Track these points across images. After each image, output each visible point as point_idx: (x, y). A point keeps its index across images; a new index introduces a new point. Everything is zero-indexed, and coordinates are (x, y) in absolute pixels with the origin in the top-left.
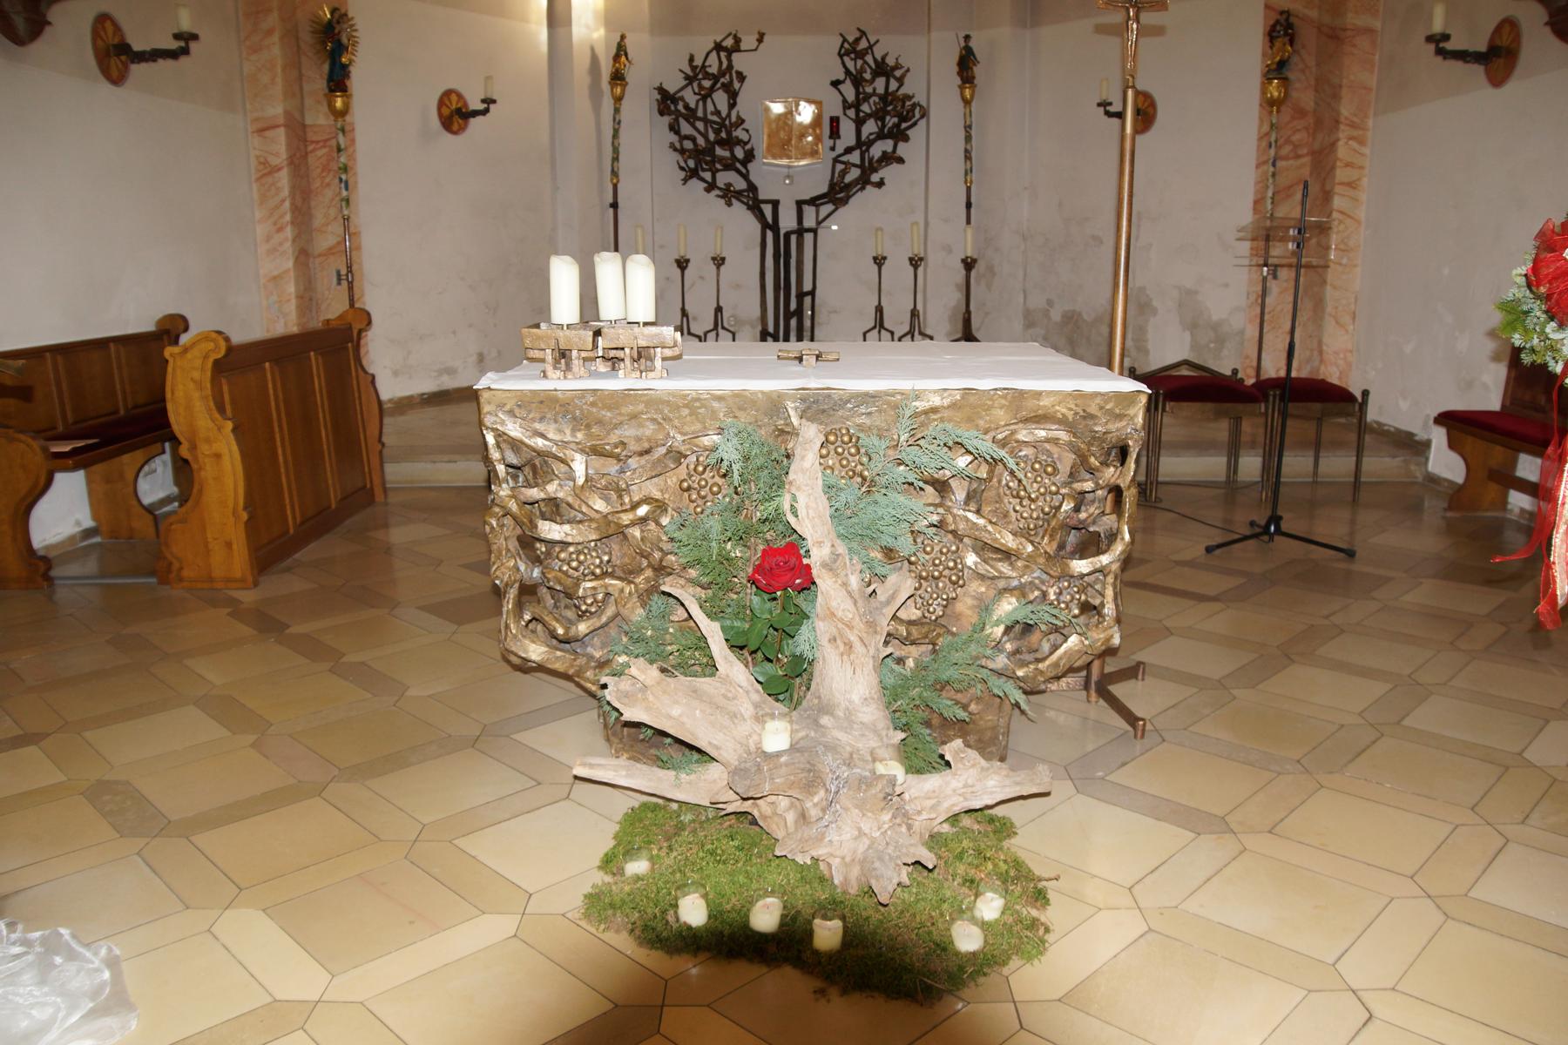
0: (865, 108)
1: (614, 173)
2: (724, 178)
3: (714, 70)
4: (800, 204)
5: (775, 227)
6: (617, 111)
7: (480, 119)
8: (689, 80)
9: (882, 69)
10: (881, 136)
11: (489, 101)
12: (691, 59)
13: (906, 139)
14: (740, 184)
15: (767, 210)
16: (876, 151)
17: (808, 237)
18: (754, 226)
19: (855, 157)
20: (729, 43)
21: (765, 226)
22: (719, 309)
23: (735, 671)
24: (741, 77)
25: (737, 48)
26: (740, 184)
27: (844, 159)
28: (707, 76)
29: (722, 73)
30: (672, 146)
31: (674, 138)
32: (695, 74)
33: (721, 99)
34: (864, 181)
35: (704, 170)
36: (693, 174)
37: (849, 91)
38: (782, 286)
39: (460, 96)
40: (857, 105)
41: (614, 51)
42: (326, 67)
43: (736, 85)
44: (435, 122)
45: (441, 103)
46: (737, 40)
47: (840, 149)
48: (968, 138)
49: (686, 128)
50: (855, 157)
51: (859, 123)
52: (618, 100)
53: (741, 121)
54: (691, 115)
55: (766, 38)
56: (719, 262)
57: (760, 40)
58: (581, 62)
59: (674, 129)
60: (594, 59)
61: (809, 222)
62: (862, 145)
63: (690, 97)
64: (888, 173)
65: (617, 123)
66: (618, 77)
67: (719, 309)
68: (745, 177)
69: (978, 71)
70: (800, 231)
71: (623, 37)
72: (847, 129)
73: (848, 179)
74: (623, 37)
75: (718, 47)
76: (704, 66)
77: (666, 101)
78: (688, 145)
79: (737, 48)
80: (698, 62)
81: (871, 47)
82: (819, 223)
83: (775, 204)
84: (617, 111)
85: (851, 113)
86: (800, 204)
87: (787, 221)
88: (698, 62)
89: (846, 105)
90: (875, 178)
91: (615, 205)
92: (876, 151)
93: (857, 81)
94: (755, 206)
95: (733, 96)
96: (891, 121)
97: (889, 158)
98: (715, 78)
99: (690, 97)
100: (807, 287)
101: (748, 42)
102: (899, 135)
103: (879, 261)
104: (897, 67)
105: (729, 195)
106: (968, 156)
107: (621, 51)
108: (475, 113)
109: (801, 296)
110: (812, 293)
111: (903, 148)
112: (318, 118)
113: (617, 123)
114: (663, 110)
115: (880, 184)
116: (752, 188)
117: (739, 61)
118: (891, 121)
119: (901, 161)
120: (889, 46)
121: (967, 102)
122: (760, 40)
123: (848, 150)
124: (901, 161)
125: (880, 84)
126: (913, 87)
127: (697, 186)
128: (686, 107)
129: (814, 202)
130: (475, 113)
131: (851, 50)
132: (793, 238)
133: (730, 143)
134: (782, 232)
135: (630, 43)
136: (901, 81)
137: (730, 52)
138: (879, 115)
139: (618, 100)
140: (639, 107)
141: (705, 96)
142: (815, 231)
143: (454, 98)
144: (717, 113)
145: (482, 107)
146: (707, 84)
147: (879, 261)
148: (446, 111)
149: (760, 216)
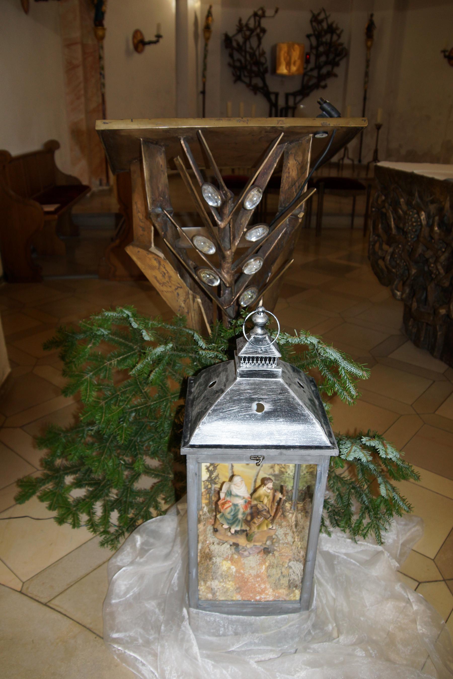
0: (321, 49)
1: (204, 76)
2: (257, 81)
4: (287, 96)
6: (206, 45)
7: (152, 47)
10: (326, 63)
11: (159, 37)
12: (240, 20)
13: (337, 64)
14: (260, 84)
15: (273, 97)
16: (324, 71)
19: (315, 73)
24: (264, 31)
25: (263, 16)
27: (310, 73)
28: (248, 29)
29: (255, 29)
30: (229, 65)
32: (241, 28)
33: (254, 42)
34: (317, 86)
35: (245, 76)
39: (141, 34)
40: (317, 48)
41: (206, 13)
42: (93, 14)
43: (261, 35)
44: (131, 47)
45: (134, 37)
46: (264, 12)
47: (309, 68)
48: (368, 66)
49: (237, 56)
51: (318, 56)
52: (207, 39)
55: (280, 12)
57: (276, 11)
59: (231, 56)
61: (291, 102)
62: (318, 67)
64: (330, 82)
66: (207, 28)
68: (264, 80)
69: (376, 33)
71: (211, 7)
72: (313, 59)
73: (311, 83)
74: (211, 7)
75: (255, 15)
76: (247, 25)
78: (238, 64)
79: (263, 15)
80: (244, 22)
81: (326, 18)
83: (277, 95)
84: (206, 45)
85: (314, 51)
86: (287, 96)
88: (244, 22)
89: (311, 47)
90: (323, 84)
91: (203, 93)
92: (324, 71)
94: (267, 94)
97: (330, 74)
98: (252, 31)
99: (240, 38)
101: (269, 12)
104: (337, 29)
105: (255, 89)
106: (367, 74)
107: (209, 14)
108: (150, 43)
111: (337, 70)
112: (91, 41)
115: (325, 87)
117: (264, 23)
118: (331, 56)
119: (336, 76)
121: (368, 48)
122: (276, 11)
123: (312, 70)
124: (336, 76)
125: (328, 37)
126: (344, 39)
128: (238, 44)
129: (295, 94)
130: (150, 43)
131: (315, 19)
133: (258, 63)
134: (279, 108)
135: (214, 10)
136: (339, 36)
139: (207, 39)
141: (247, 39)
143: (139, 34)
144: (251, 48)
145: (154, 39)
146: (248, 33)
148: (136, 41)
149: (269, 100)
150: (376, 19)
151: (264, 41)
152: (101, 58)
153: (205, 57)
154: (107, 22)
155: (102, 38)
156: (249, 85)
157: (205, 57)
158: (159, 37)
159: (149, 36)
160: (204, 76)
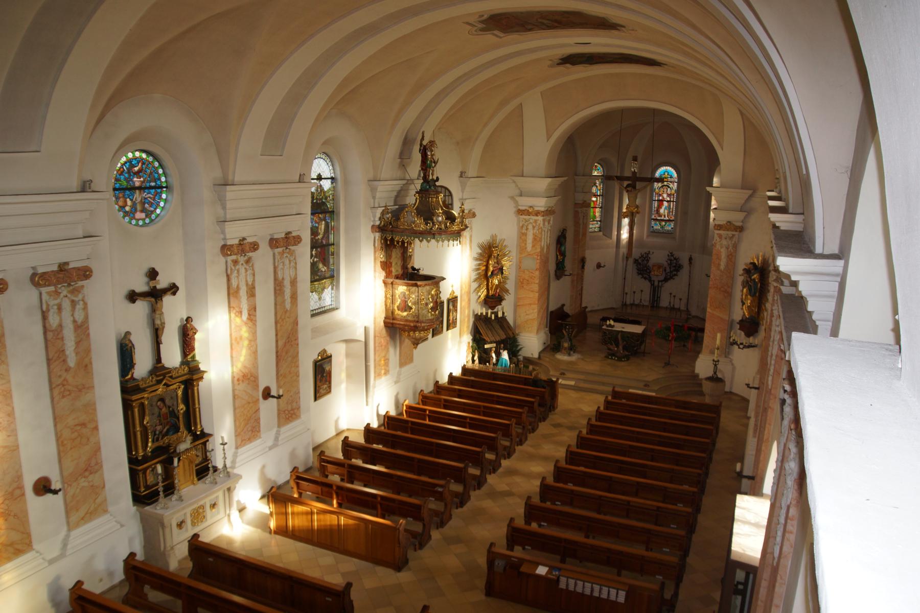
3: (644, 256)
4: (659, 281)
5: (654, 284)
8: (640, 258)
9: (675, 259)
10: (675, 270)
11: (604, 266)
12: (641, 254)
13: (679, 271)
14: (648, 277)
15: (653, 282)
17: (660, 288)
18: (649, 284)
20: (648, 252)
21: (652, 285)
22: (641, 300)
23: (614, 345)
24: (650, 258)
26: (648, 277)
29: (646, 257)
31: (636, 267)
32: (642, 256)
34: (669, 279)
36: (639, 274)
37: (669, 262)
38: (654, 296)
44: (596, 267)
45: (598, 264)
46: (649, 252)
48: (690, 273)
49: (639, 266)
50: (669, 274)
51: (670, 268)
52: (627, 261)
53: (649, 266)
54: (640, 264)
56: (642, 291)
57: (653, 253)
58: (621, 254)
60: (624, 254)
61: (660, 284)
62: (671, 272)
63: (640, 261)
65: (626, 264)
67: (641, 300)
68: (649, 276)
69: (693, 261)
70: (658, 286)
72: (668, 270)
75: (646, 253)
76: (643, 255)
77: (636, 261)
82: (662, 284)
83: (654, 281)
86: (659, 281)
87: (656, 283)
89: (668, 264)
91: (625, 279)
93: (671, 260)
94: (650, 281)
95: (648, 261)
96: (677, 268)
97: (676, 275)
98: (645, 258)
100: (659, 296)
101: (651, 253)
102: (678, 271)
103: (671, 294)
105: (645, 278)
106: (690, 276)
109: (657, 297)
110: (660, 297)
111: (679, 273)
113: (626, 264)
114: (635, 263)
115: (674, 279)
116: (650, 277)
118: (677, 268)
120: (676, 254)
121: (690, 266)
122: (653, 253)
123: (668, 273)
125: (675, 261)
127: (640, 276)
129: (662, 281)
131: (672, 254)
132: (657, 288)
137: (648, 254)
138: (675, 267)
139: (627, 261)
140: (631, 261)
141: (643, 261)
142: (661, 287)
147: (671, 294)
149: (651, 283)
150: (692, 257)
151: (650, 262)
152: (582, 276)
153: (626, 267)
154: (585, 267)
155: (583, 272)
156: (643, 277)
157: (626, 267)
158: (604, 266)
159: (602, 265)
160: (625, 273)
